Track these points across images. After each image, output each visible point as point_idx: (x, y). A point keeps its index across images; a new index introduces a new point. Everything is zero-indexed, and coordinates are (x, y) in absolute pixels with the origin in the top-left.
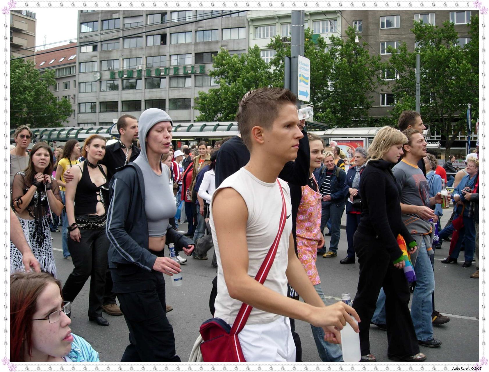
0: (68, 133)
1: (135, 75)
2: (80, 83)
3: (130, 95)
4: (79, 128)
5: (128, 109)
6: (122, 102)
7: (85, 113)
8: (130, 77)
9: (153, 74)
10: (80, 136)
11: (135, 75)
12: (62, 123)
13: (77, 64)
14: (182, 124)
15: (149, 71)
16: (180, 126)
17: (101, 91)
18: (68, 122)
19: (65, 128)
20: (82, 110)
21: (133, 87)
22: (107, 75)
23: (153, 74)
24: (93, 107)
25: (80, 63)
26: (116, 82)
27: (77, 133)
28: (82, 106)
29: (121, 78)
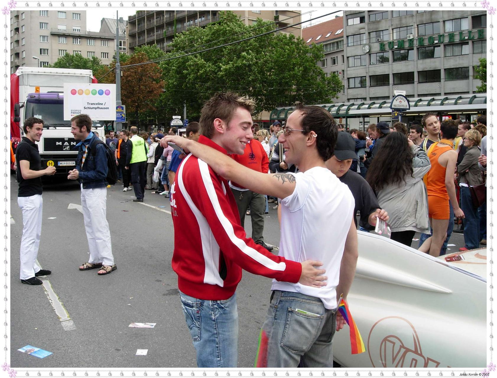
0: (339, 110)
1: (407, 45)
2: (348, 57)
3: (401, 67)
4: (349, 104)
5: (399, 82)
6: (394, 74)
7: (355, 88)
8: (401, 48)
9: (426, 43)
10: (351, 112)
11: (407, 45)
12: (332, 100)
13: (345, 38)
14: (463, 96)
15: (421, 40)
16: (460, 98)
17: (370, 64)
18: (337, 98)
19: (336, 104)
20: (352, 85)
21: (405, 58)
22: (376, 47)
23: (426, 43)
24: (363, 83)
25: (348, 37)
26: (386, 55)
27: (348, 109)
28: (351, 81)
29: (392, 49)
